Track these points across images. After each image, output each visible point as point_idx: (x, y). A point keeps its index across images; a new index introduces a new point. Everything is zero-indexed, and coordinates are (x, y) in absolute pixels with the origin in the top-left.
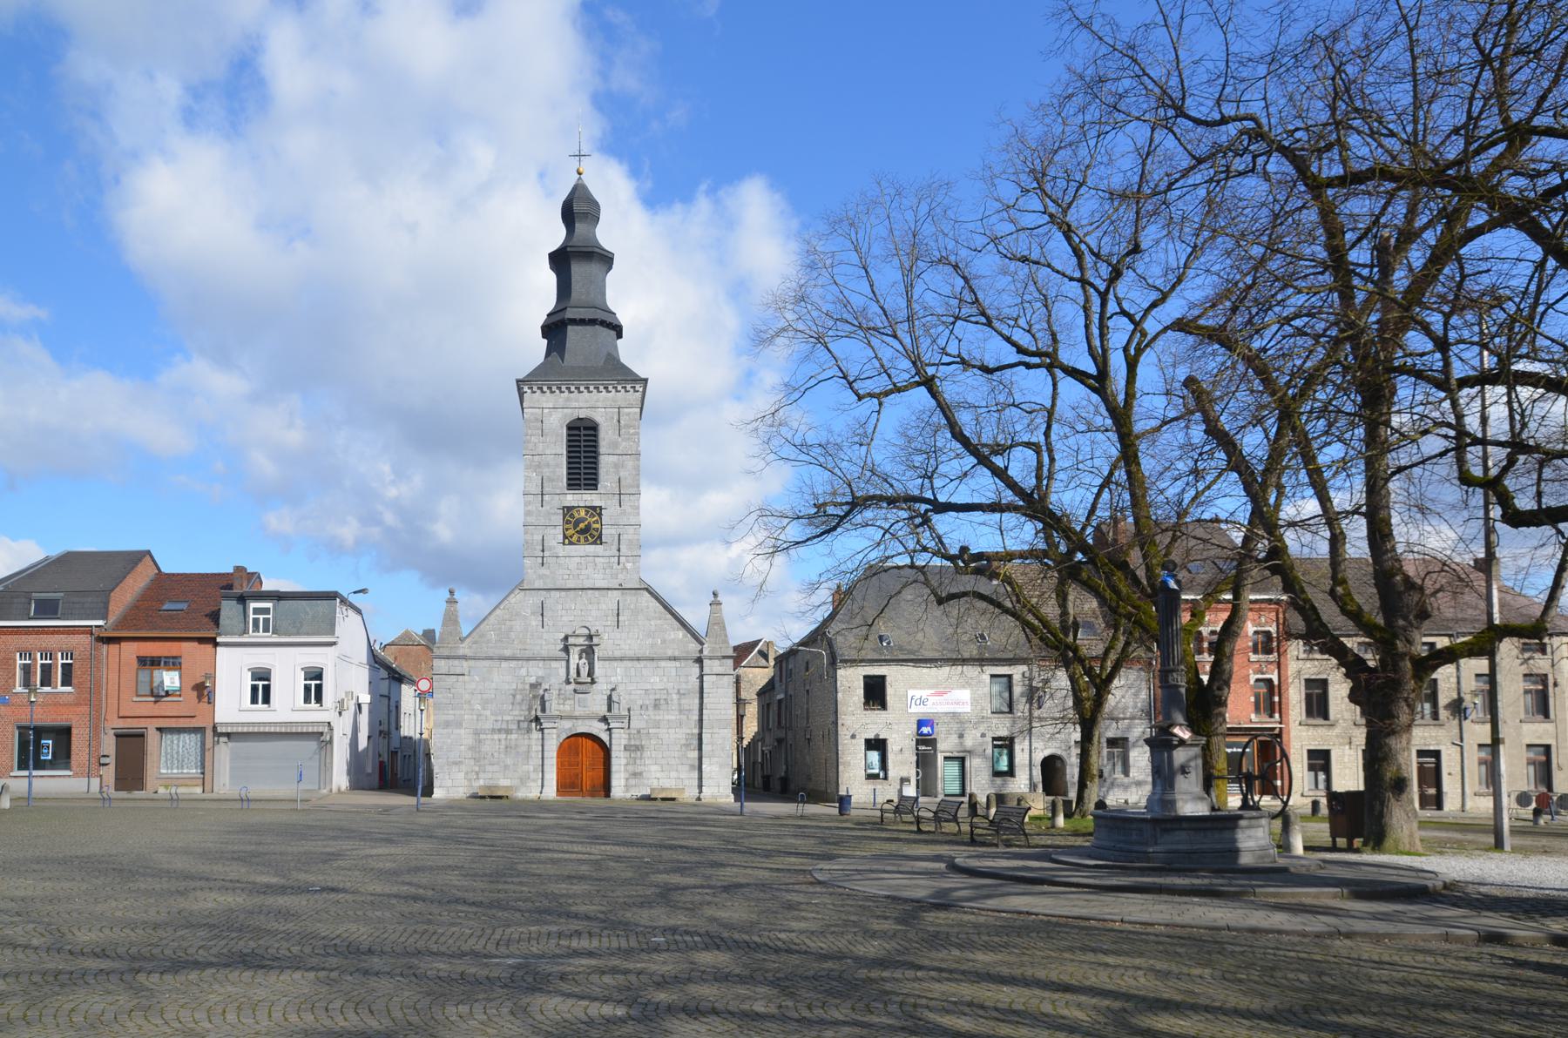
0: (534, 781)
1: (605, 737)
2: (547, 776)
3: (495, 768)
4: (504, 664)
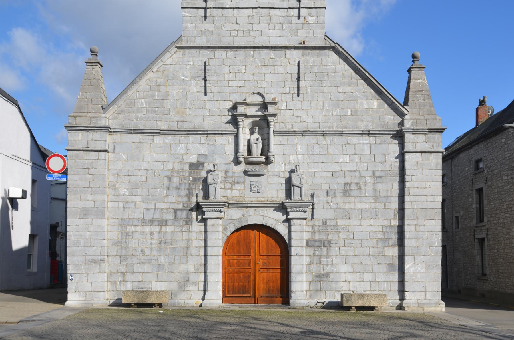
0: (195, 284)
1: (282, 230)
2: (210, 278)
3: (147, 268)
4: (158, 139)
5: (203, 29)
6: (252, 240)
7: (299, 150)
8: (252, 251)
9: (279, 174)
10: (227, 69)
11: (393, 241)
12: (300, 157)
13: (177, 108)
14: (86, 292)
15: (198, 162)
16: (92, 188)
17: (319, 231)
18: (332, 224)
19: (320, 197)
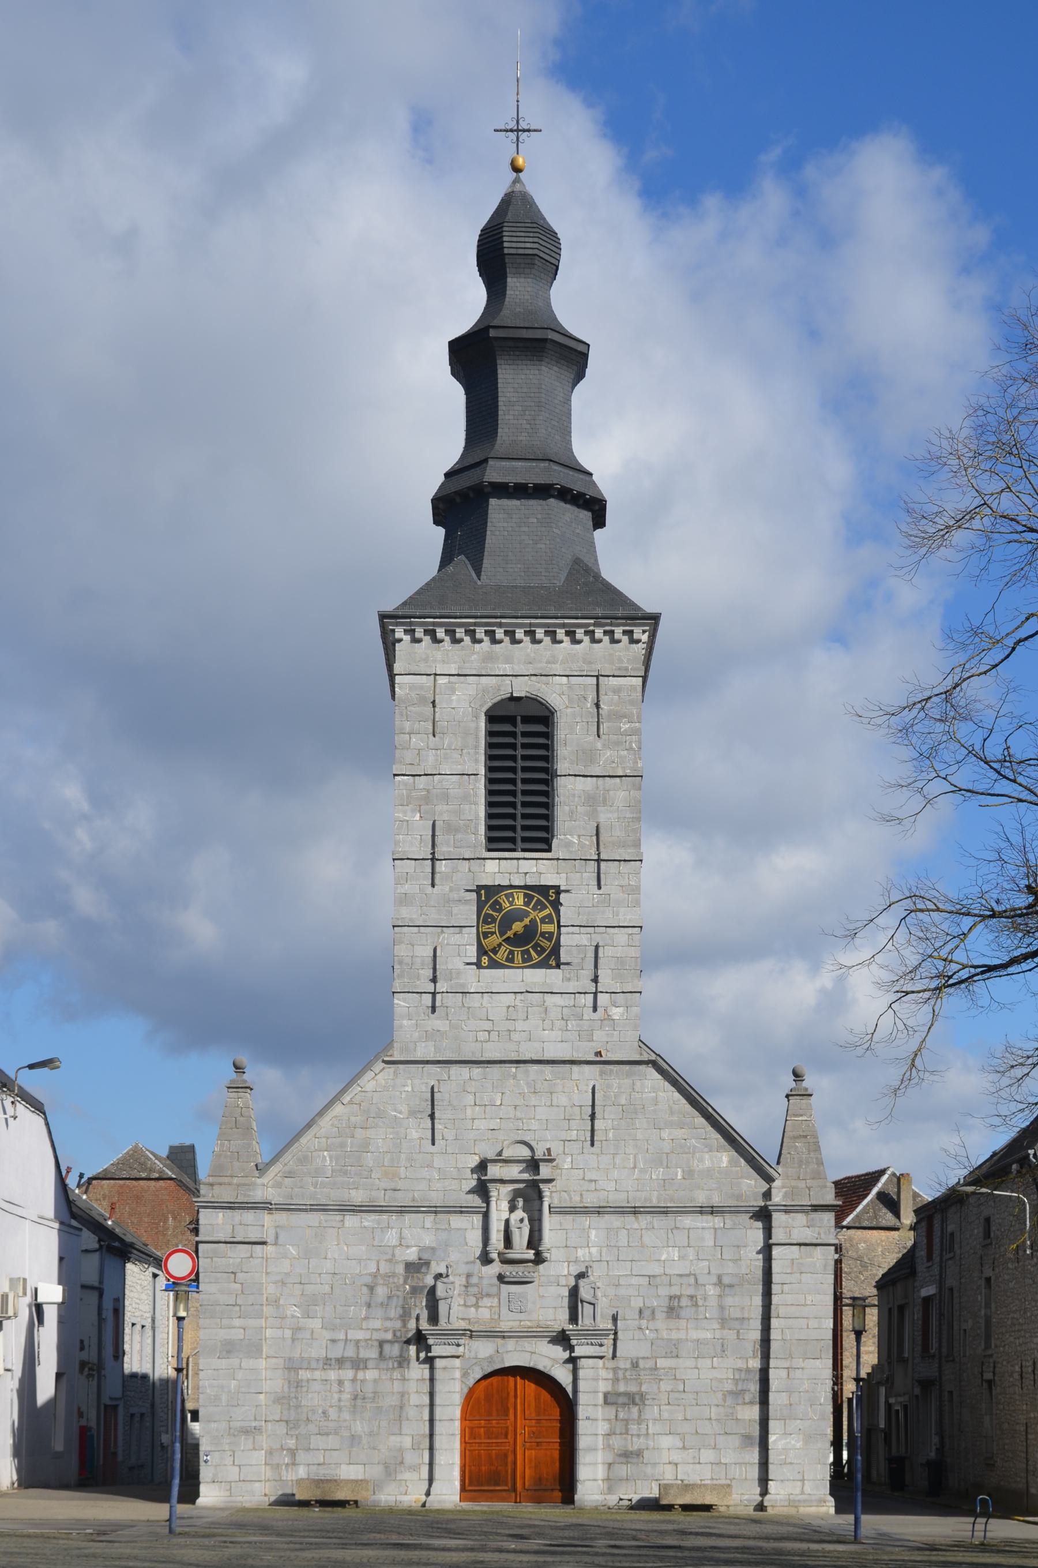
0: (415, 1468)
1: (563, 1375)
2: (440, 1458)
3: (332, 1441)
4: (351, 1221)
5: (429, 1029)
6: (512, 1393)
8: (511, 1411)
10: (470, 1099)
11: (751, 1396)
12: (594, 1250)
13: (384, 1166)
14: (231, 1482)
15: (420, 1259)
16: (240, 1306)
17: (625, 1378)
18: (647, 1367)
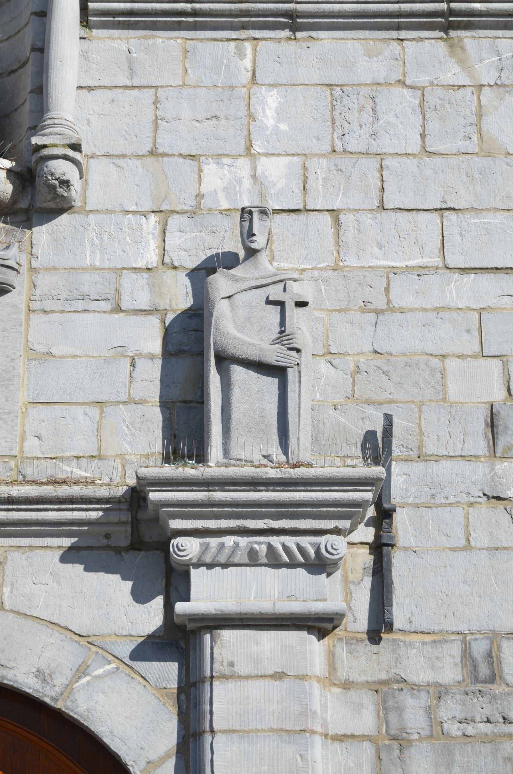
7: (270, 122)
9: (118, 291)
19: (437, 458)
